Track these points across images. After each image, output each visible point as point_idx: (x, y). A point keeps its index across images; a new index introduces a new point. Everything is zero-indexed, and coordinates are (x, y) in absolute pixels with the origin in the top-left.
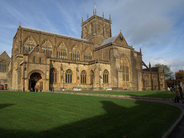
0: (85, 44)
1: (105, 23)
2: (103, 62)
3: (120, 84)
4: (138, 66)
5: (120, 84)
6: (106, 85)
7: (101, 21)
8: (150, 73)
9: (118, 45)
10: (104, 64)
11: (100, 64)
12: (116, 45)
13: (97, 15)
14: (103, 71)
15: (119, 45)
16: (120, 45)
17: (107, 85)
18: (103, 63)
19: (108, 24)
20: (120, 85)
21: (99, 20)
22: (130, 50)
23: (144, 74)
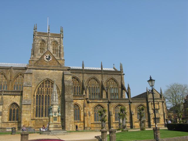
0: (16, 70)
1: (52, 38)
2: (10, 93)
3: (26, 121)
4: (68, 94)
5: (25, 122)
6: (12, 124)
7: (45, 37)
8: (107, 101)
9: (38, 68)
10: (11, 96)
11: (4, 96)
12: (34, 68)
13: (38, 31)
14: (9, 105)
15: (40, 68)
16: (42, 68)
17: (15, 123)
18: (10, 95)
19: (56, 39)
20: (25, 123)
21: (41, 37)
22: (62, 71)
23: (112, 104)
